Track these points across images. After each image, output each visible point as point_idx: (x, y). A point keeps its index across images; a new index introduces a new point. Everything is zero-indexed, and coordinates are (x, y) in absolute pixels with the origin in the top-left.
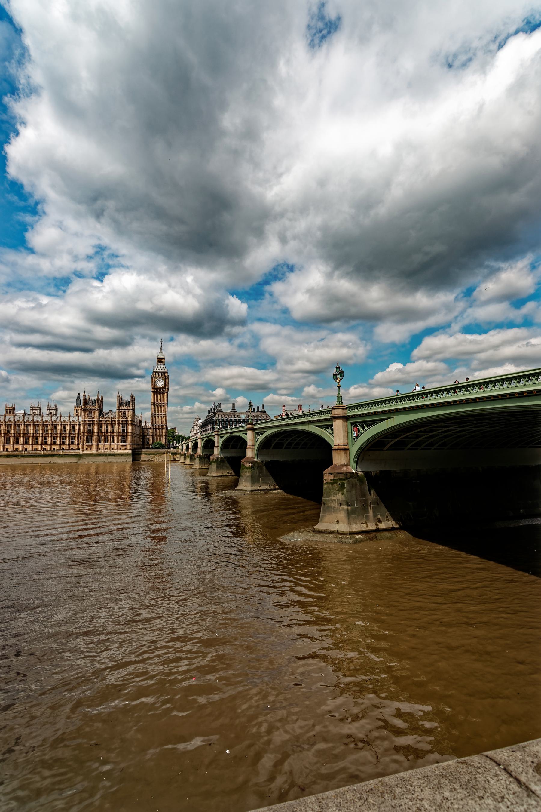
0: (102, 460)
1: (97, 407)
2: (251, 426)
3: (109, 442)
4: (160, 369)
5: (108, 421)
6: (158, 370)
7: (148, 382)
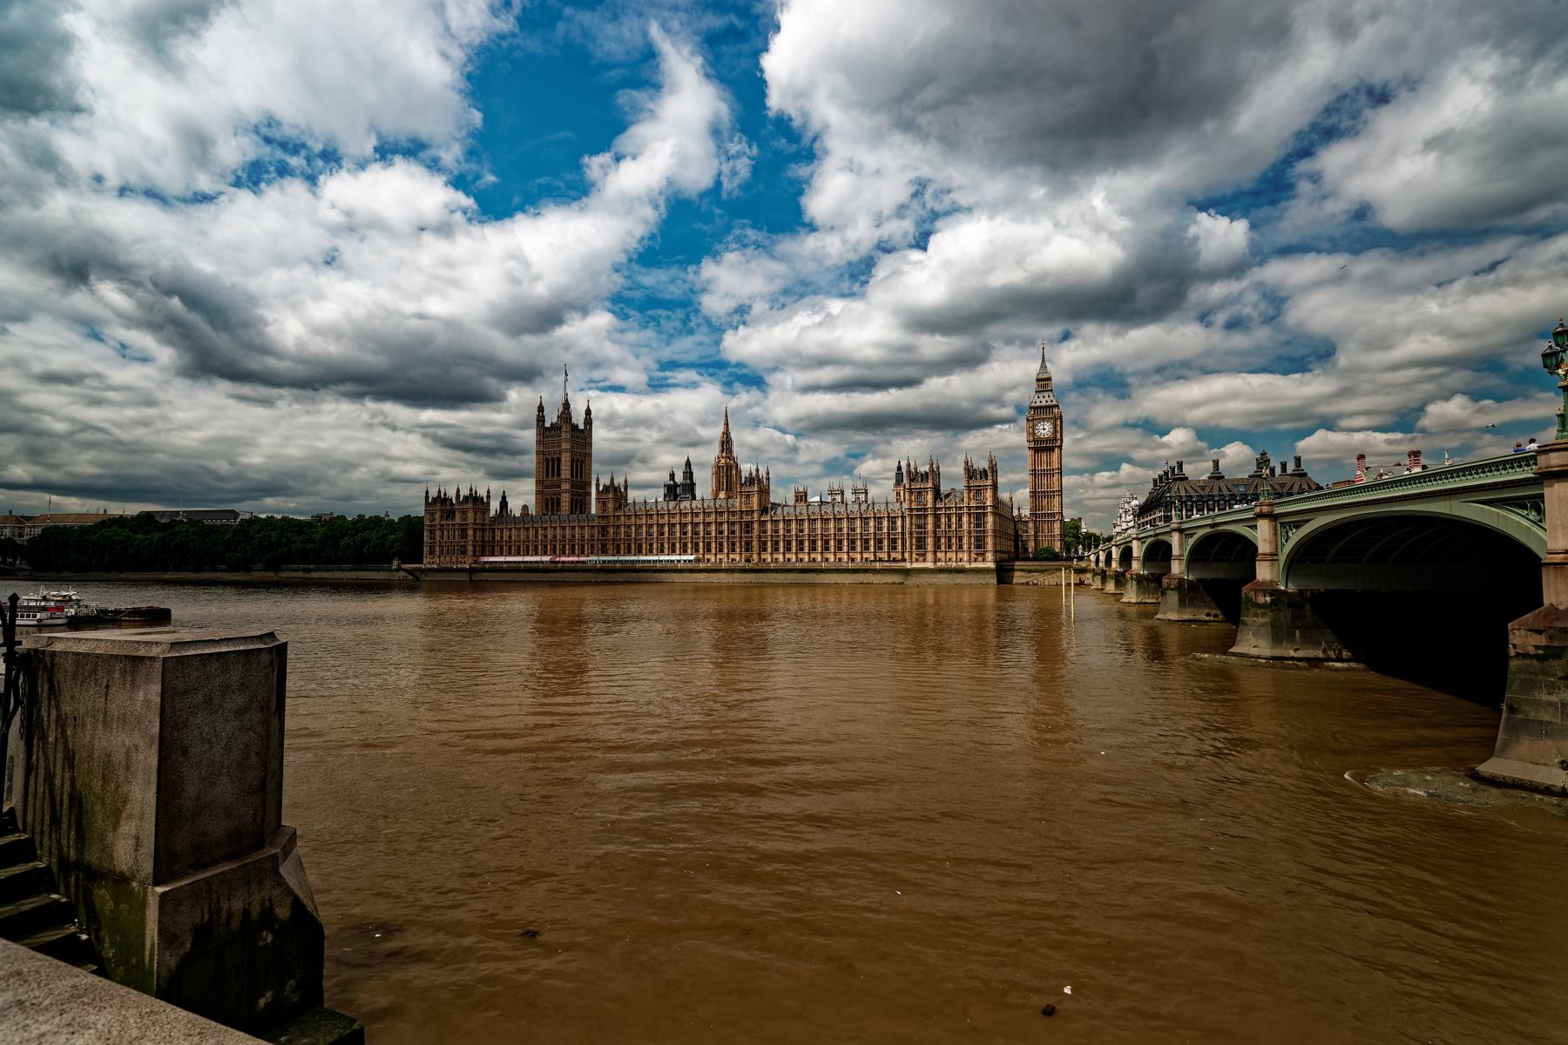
1: (930, 485)
2: (1265, 509)
4: (1044, 401)
5: (950, 508)
6: (1038, 404)
7: (1021, 430)
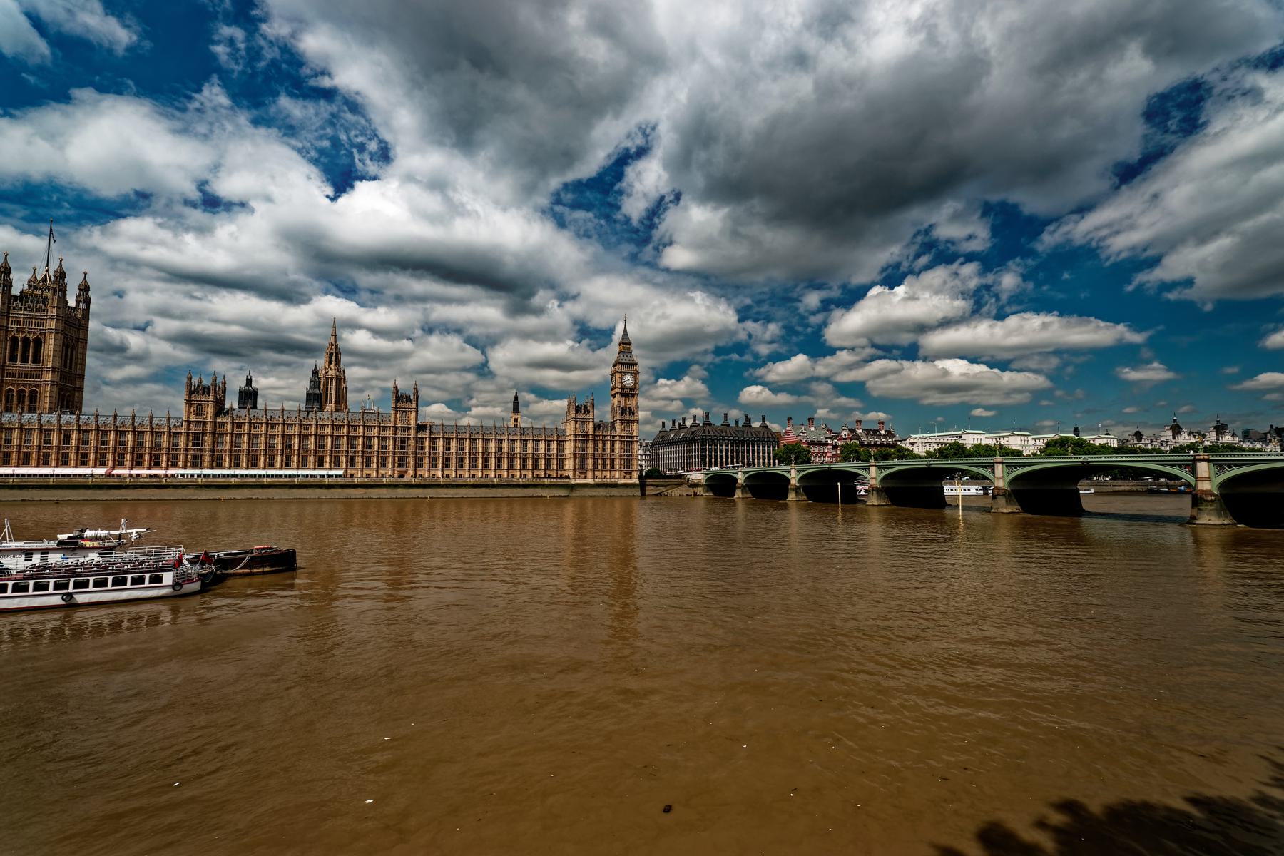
0: (602, 493)
3: (608, 467)
5: (605, 436)
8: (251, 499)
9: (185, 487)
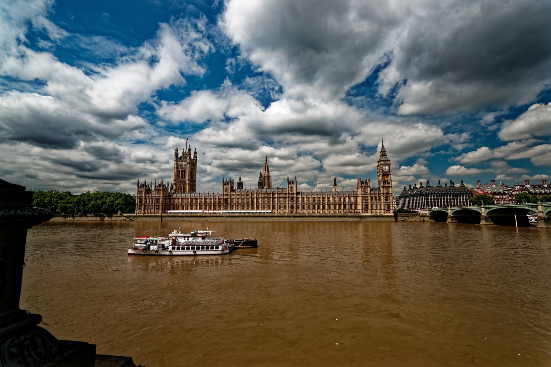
0: (376, 220)
3: (378, 208)
4: (385, 159)
8: (242, 221)
9: (223, 217)
